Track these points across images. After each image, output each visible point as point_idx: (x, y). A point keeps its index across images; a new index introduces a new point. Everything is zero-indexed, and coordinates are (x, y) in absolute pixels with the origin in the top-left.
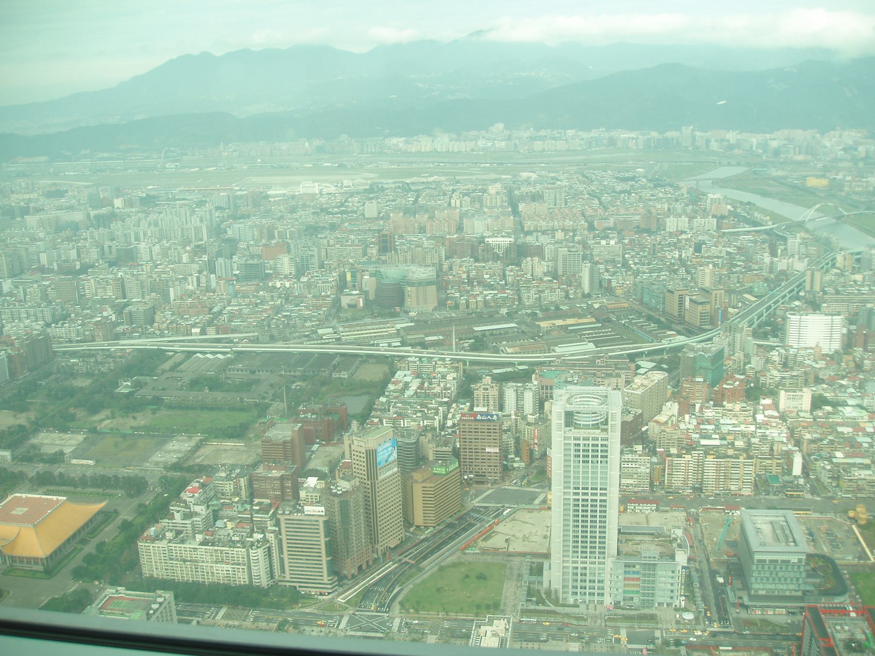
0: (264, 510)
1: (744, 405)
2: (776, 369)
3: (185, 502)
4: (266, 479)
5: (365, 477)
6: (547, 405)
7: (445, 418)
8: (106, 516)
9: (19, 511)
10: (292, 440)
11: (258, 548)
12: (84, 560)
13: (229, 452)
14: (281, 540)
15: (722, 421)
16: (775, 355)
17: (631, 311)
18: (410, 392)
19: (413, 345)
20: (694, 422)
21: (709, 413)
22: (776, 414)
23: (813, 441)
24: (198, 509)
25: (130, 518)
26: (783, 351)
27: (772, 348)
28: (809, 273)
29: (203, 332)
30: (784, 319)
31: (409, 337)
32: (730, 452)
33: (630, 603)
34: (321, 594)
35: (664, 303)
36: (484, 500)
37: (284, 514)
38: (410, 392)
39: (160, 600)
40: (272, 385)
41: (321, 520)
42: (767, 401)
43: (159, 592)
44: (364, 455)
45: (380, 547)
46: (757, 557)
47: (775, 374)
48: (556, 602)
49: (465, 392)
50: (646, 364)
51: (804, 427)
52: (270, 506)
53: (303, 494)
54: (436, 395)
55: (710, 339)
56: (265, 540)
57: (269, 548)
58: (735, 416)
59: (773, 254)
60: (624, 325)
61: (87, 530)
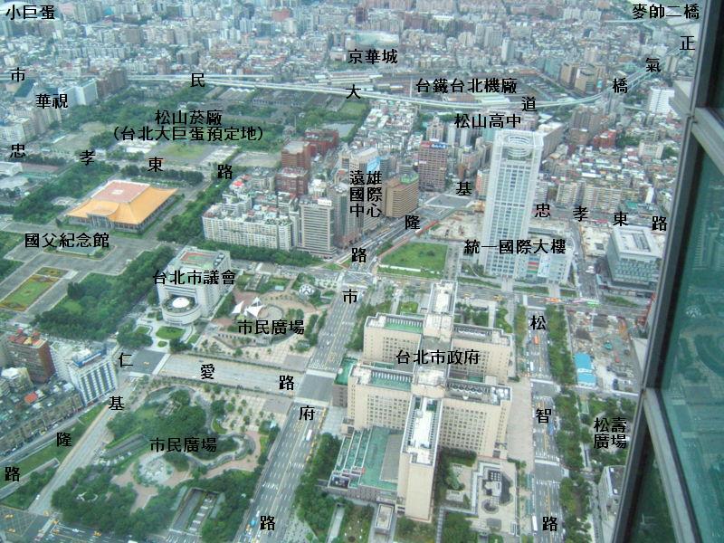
0: (286, 200)
1: (614, 151)
2: (638, 127)
3: (233, 191)
4: (287, 179)
6: (478, 141)
7: (406, 143)
8: (177, 199)
9: (117, 192)
10: (303, 153)
13: (258, 160)
15: (597, 161)
16: (638, 117)
17: (536, 76)
18: (381, 125)
19: (382, 91)
20: (578, 160)
21: (589, 155)
22: (636, 159)
23: (662, 181)
24: (242, 196)
25: (193, 200)
26: (644, 115)
27: (636, 111)
28: (668, 58)
29: (234, 72)
30: (647, 90)
31: (380, 85)
32: (605, 183)
33: (530, 279)
34: (325, 258)
35: (560, 72)
36: (432, 203)
38: (381, 125)
39: (222, 256)
40: (285, 114)
41: (329, 210)
42: (631, 150)
43: (220, 251)
45: (364, 229)
46: (622, 256)
47: (637, 130)
48: (481, 274)
49: (419, 128)
50: (546, 117)
51: (656, 170)
52: (290, 197)
54: (401, 128)
55: (593, 102)
56: (289, 221)
57: (291, 226)
58: (608, 158)
59: (642, 41)
60: (530, 87)
61: (165, 207)
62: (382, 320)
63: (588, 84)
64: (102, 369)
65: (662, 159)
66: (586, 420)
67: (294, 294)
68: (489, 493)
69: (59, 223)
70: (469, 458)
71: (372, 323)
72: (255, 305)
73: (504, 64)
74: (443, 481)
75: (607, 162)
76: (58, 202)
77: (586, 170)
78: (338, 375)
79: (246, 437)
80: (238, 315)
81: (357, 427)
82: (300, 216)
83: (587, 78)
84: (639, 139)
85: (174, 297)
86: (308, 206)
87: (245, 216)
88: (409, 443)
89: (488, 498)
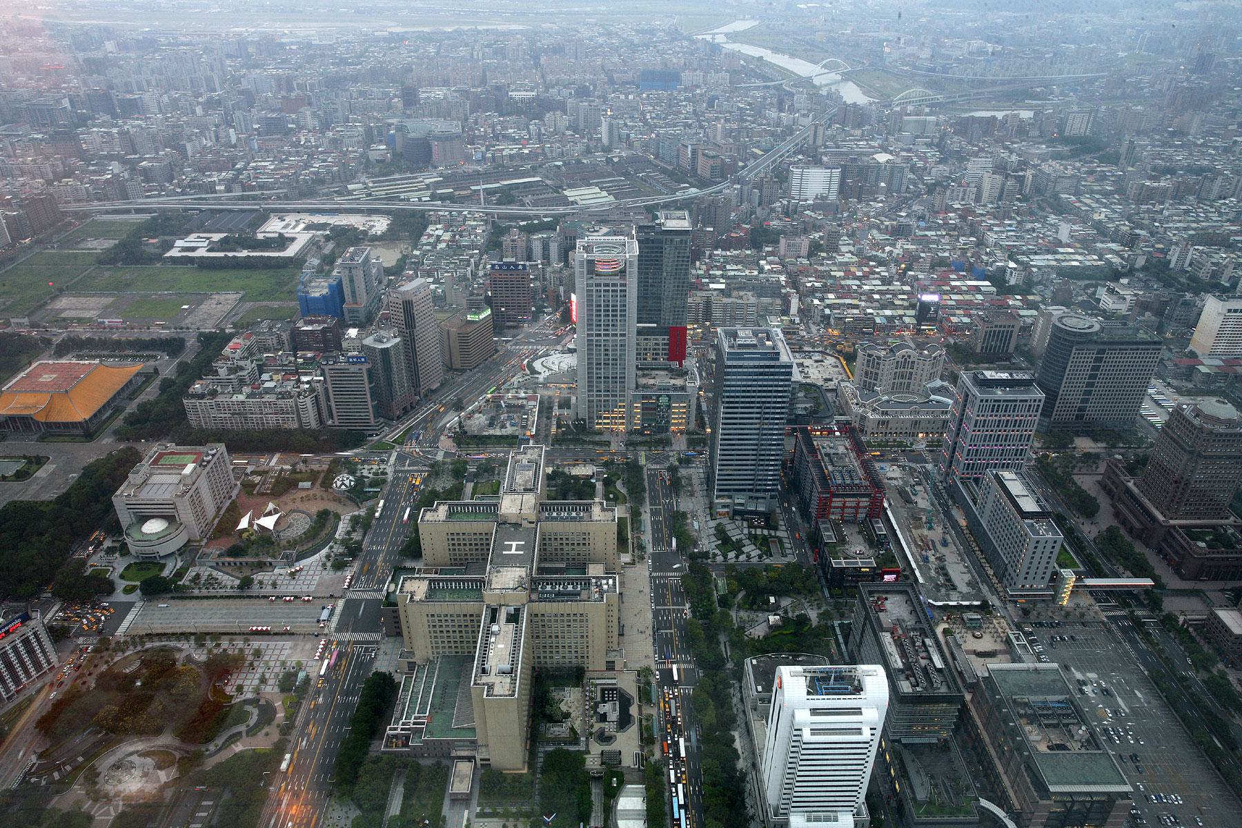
8: (148, 377)
12: (125, 419)
15: (728, 267)
20: (704, 267)
24: (242, 363)
29: (228, 190)
30: (788, 171)
41: (365, 367)
47: (775, 224)
49: (494, 244)
53: (344, 345)
59: (781, 110)
62: (443, 510)
63: (713, 168)
64: (26, 642)
65: (809, 256)
66: (725, 602)
68: (603, 718)
70: (576, 676)
71: (429, 516)
72: (270, 514)
73: (607, 150)
74: (540, 709)
75: (739, 267)
77: (713, 279)
79: (262, 702)
80: (244, 530)
81: (418, 659)
83: (711, 162)
84: (779, 233)
85: (144, 519)
86: (336, 367)
87: (247, 390)
88: (484, 671)
89: (602, 725)
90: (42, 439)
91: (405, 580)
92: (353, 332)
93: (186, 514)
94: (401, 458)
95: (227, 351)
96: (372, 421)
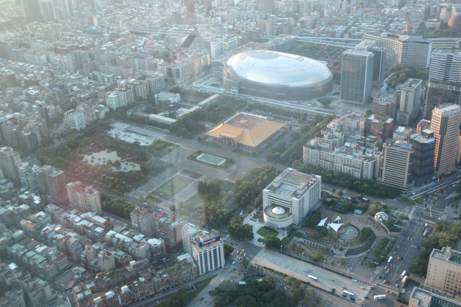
3: (330, 129)
5: (438, 132)
9: (243, 121)
10: (392, 104)
11: (369, 161)
14: (383, 159)
24: (337, 134)
37: (387, 145)
39: (315, 180)
41: (409, 152)
44: (440, 120)
53: (395, 135)
64: (215, 251)
67: (370, 218)
69: (200, 140)
71: (437, 255)
72: (336, 222)
76: (201, 123)
78: (401, 294)
80: (321, 227)
82: (384, 156)
85: (274, 205)
86: (392, 148)
87: (337, 150)
90: (234, 151)
91: (417, 290)
92: (401, 129)
93: (295, 211)
94: (417, 214)
95: (331, 125)
96: (405, 185)
